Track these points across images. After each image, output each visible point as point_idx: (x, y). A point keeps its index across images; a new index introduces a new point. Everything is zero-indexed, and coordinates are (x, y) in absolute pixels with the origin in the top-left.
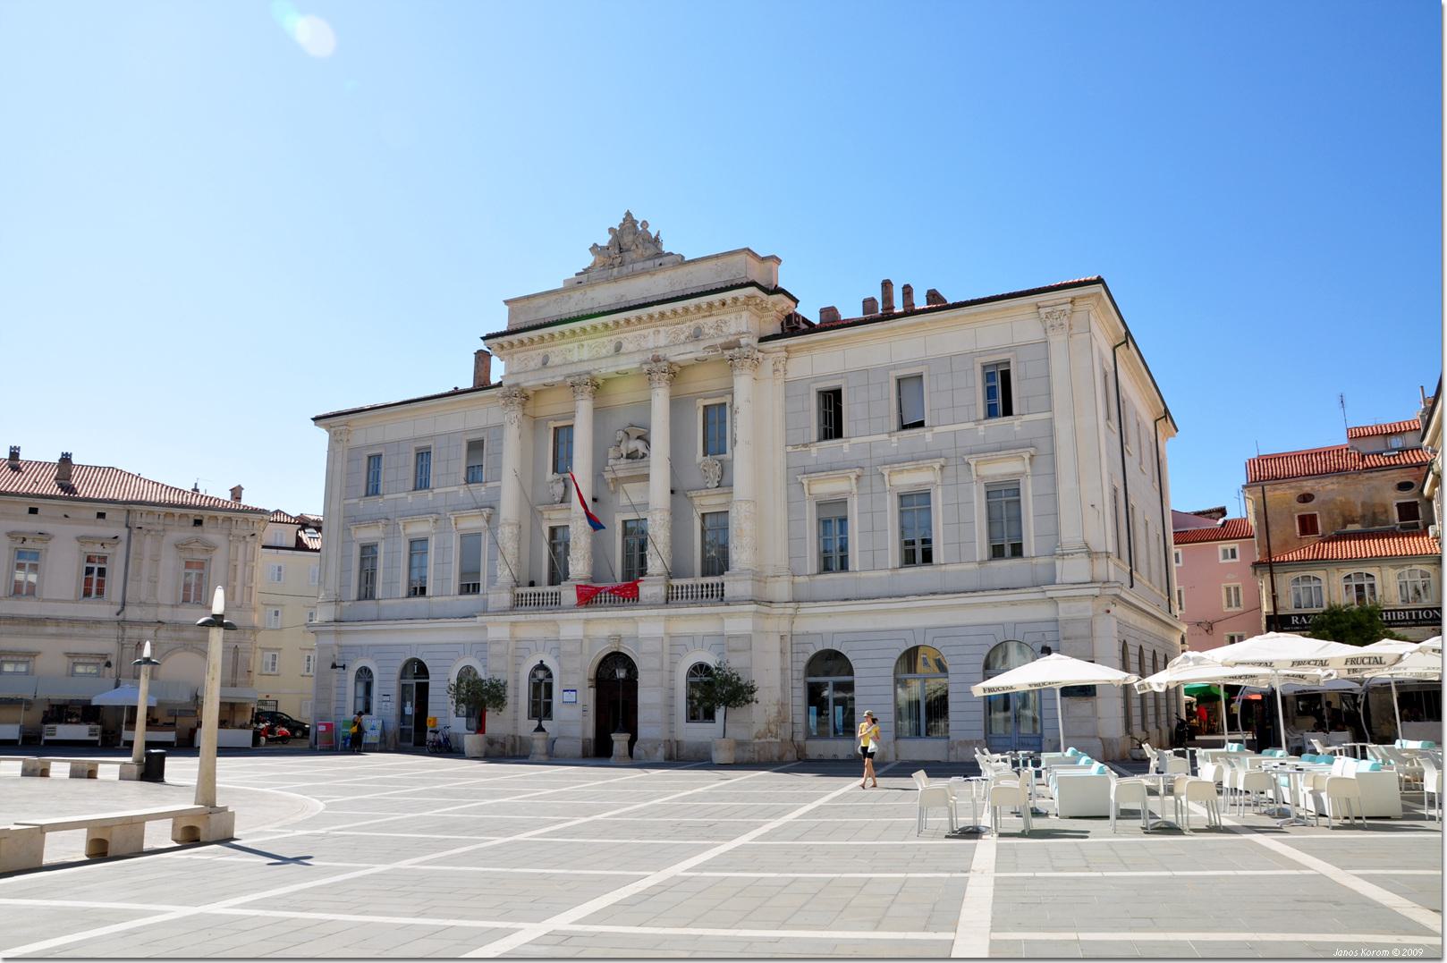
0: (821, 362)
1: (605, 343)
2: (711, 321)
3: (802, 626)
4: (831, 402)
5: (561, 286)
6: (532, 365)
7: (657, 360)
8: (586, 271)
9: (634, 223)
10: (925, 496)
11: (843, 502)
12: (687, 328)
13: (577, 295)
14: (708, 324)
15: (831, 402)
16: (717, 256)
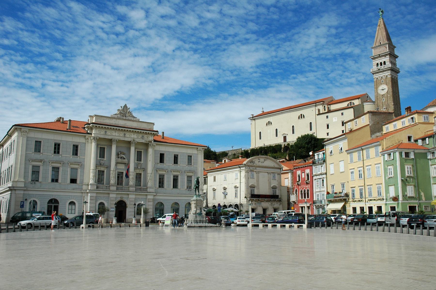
0: (162, 149)
1: (122, 134)
2: (146, 136)
3: (157, 197)
4: (162, 156)
5: (110, 116)
6: (102, 133)
7: (134, 140)
8: (115, 114)
9: (127, 107)
10: (177, 176)
11: (164, 175)
12: (140, 135)
13: (114, 120)
14: (145, 136)
15: (162, 156)
16: (148, 123)
